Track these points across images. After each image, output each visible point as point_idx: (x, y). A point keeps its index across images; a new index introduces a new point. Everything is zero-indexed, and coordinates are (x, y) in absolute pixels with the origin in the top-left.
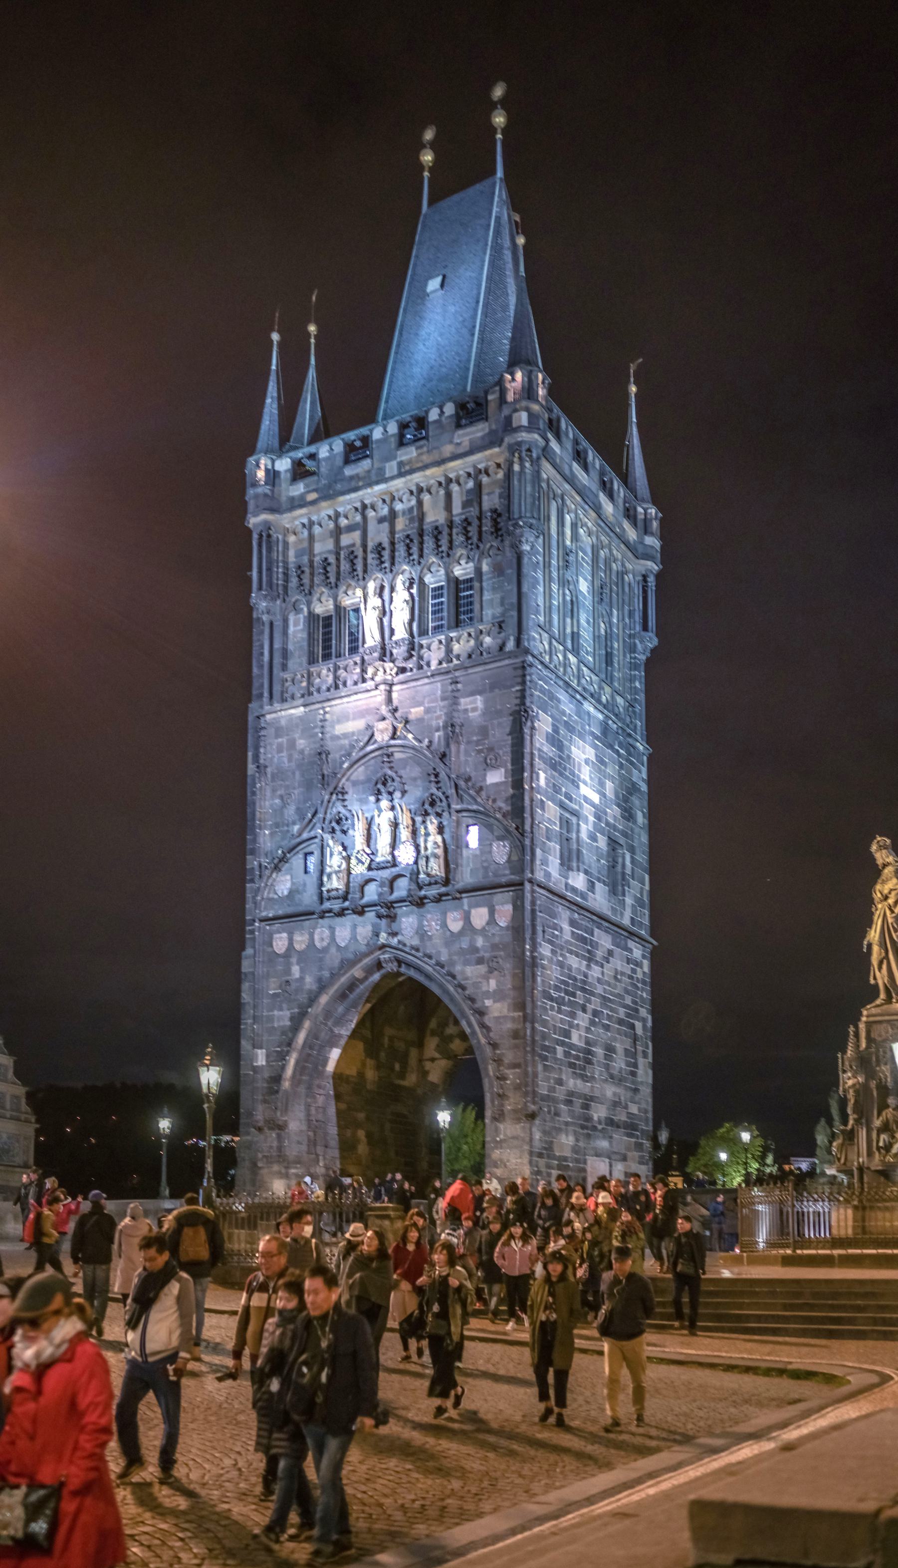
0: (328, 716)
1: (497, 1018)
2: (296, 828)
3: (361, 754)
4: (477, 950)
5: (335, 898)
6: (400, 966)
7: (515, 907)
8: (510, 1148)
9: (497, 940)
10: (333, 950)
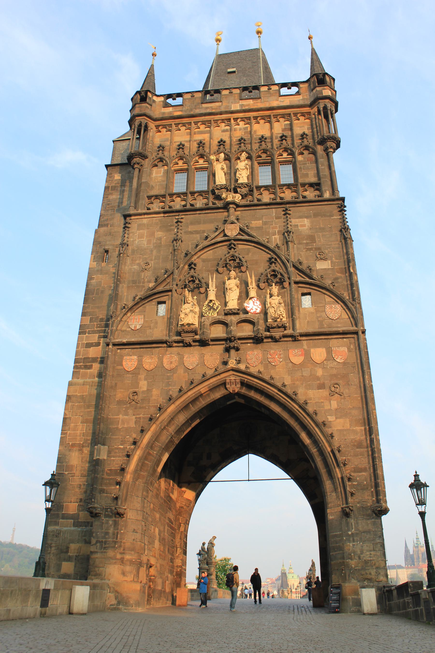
0: (182, 220)
1: (340, 431)
2: (151, 285)
3: (213, 241)
4: (318, 378)
5: (187, 332)
6: (241, 388)
7: (349, 350)
8: (364, 542)
9: (334, 372)
10: (181, 371)
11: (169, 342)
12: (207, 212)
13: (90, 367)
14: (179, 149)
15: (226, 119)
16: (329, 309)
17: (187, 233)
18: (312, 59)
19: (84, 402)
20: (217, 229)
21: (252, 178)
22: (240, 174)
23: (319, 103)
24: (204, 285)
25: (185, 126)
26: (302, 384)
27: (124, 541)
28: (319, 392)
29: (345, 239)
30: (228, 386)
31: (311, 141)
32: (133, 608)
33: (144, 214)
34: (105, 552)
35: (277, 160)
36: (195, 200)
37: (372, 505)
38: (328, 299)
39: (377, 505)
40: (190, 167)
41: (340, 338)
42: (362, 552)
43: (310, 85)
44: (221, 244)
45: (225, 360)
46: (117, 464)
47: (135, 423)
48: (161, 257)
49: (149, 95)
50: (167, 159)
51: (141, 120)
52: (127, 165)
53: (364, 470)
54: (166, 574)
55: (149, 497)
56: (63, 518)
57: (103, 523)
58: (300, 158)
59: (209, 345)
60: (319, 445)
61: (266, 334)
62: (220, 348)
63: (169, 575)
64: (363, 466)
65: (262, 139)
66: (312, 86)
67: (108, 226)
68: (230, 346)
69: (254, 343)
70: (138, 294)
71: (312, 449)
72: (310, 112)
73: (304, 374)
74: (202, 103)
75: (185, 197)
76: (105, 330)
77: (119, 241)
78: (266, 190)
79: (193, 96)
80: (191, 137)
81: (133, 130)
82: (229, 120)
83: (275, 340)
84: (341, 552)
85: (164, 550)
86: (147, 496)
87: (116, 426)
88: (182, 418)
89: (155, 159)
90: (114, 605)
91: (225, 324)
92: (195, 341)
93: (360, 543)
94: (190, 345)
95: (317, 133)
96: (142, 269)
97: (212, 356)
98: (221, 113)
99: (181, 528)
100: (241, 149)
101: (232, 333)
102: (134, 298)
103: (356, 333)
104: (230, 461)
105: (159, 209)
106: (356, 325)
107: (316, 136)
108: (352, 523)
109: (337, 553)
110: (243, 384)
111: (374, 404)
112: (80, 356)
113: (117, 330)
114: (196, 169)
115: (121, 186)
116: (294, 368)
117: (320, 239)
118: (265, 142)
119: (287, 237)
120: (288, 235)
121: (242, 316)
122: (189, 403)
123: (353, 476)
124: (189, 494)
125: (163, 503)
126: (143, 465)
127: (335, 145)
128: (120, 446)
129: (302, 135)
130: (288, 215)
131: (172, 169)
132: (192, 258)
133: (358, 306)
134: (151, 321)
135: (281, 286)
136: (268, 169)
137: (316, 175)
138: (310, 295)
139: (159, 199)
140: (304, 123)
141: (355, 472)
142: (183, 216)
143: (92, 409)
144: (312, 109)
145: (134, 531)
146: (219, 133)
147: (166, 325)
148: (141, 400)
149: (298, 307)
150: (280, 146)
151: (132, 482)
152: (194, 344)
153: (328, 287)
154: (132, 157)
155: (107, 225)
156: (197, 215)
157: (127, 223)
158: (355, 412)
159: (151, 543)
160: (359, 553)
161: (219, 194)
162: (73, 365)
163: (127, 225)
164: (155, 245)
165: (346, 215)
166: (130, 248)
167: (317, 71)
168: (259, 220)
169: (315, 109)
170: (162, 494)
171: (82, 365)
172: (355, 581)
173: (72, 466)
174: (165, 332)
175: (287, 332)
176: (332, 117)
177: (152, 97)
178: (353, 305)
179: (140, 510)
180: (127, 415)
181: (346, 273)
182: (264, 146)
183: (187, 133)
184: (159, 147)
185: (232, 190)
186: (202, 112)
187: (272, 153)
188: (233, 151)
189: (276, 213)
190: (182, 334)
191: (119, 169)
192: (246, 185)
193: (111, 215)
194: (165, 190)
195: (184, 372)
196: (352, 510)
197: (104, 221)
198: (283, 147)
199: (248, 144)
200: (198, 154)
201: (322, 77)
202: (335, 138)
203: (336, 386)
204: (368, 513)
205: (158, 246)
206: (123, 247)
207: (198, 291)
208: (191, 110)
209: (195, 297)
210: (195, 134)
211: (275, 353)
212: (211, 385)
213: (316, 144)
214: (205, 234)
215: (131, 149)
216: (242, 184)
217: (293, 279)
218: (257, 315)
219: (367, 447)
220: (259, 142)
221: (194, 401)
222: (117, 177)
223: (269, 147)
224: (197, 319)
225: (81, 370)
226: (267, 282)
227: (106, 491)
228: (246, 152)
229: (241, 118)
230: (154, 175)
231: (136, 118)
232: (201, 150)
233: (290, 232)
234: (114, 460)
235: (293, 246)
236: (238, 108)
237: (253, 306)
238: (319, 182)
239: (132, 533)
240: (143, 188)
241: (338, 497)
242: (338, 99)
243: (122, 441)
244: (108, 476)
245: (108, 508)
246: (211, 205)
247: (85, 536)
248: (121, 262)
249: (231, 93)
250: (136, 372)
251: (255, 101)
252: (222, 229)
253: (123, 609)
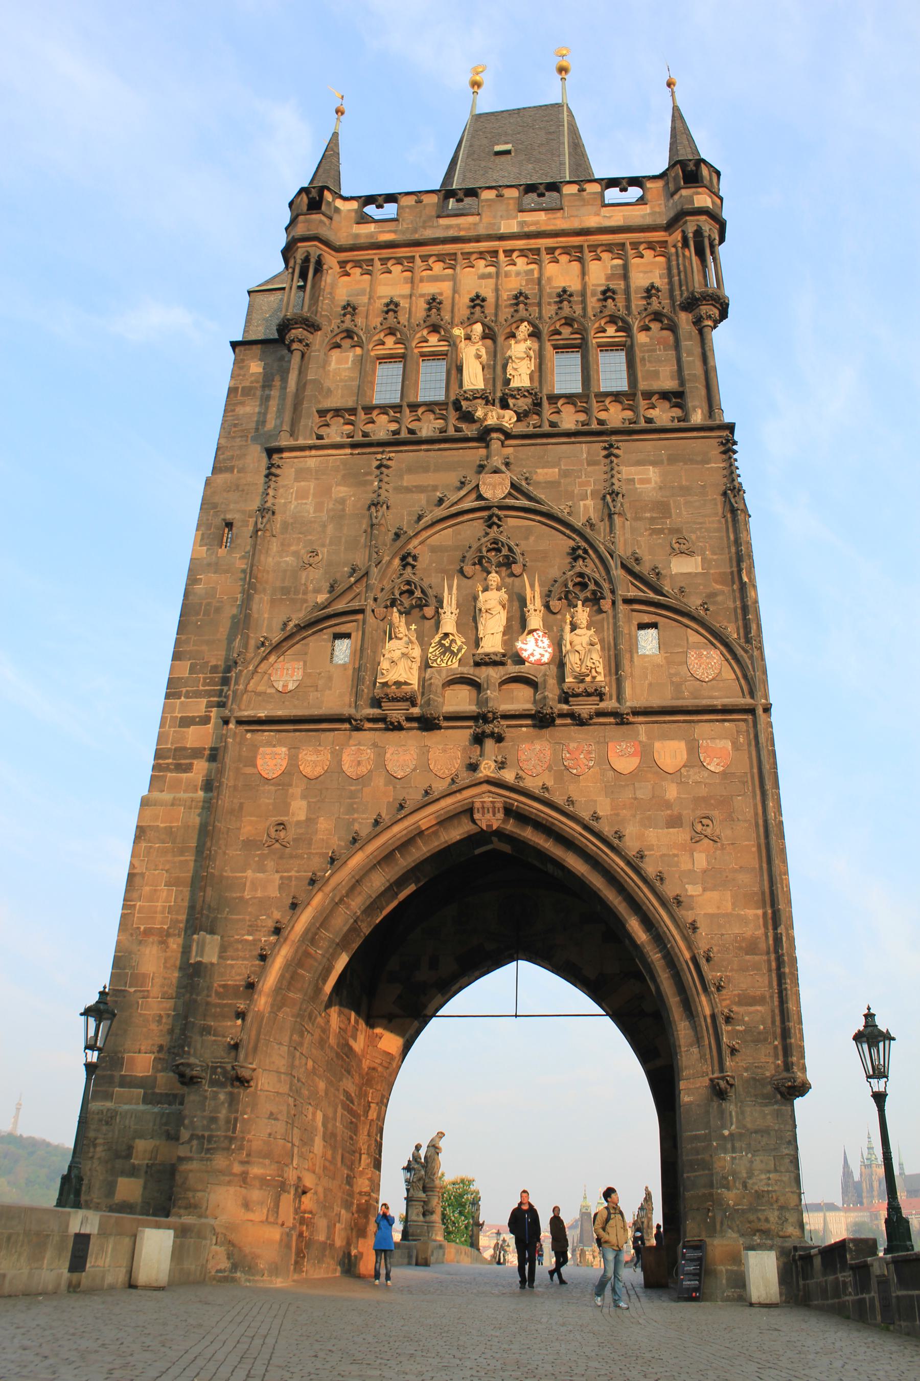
0: (389, 463)
2: (321, 598)
3: (454, 510)
4: (668, 805)
5: (395, 699)
6: (505, 821)
7: (736, 746)
8: (755, 1152)
9: (703, 791)
10: (379, 781)
11: (356, 720)
12: (442, 446)
13: (188, 768)
14: (387, 312)
15: (488, 252)
16: (696, 659)
17: (399, 490)
18: (673, 129)
19: (174, 842)
20: (463, 483)
21: (540, 376)
22: (516, 369)
23: (686, 222)
24: (432, 601)
25: (401, 264)
26: (635, 816)
27: (250, 1136)
28: (668, 833)
29: (733, 511)
30: (477, 816)
31: (666, 302)
32: (265, 1278)
33: (311, 448)
34: (208, 1159)
35: (594, 341)
36: (419, 420)
37: (774, 1076)
38: (694, 638)
39: (785, 1075)
40: (409, 351)
41: (717, 721)
42: (750, 1174)
43: (667, 184)
44: (471, 516)
45: (473, 761)
46: (239, 974)
47: (280, 888)
48: (343, 540)
49: (328, 196)
50: (361, 333)
51: (308, 249)
52: (276, 343)
53: (761, 1000)
54: (337, 1209)
55: (305, 1045)
56: (121, 1085)
57: (206, 1098)
58: (642, 338)
59: (440, 728)
60: (665, 946)
61: (561, 708)
62: (463, 736)
63: (343, 1212)
64: (758, 993)
65: (564, 295)
66: (672, 187)
67: (232, 472)
68: (483, 732)
69: (534, 726)
70: (294, 617)
71: (651, 954)
72: (666, 242)
73: (640, 795)
74: (439, 217)
75: (398, 415)
76: (222, 691)
77: (256, 504)
78: (568, 403)
79: (421, 202)
80: (412, 288)
81: (290, 270)
82: (495, 253)
83: (579, 721)
84: (707, 1172)
85: (334, 1158)
86: (301, 1044)
87: (238, 895)
88: (378, 881)
89: (335, 333)
90: (225, 1271)
91: (476, 685)
92: (409, 719)
93: (746, 1155)
94: (399, 728)
95: (681, 286)
96: (302, 564)
97: (446, 752)
98: (478, 239)
99: (370, 1112)
100: (518, 316)
101: (490, 704)
102: (285, 625)
103: (751, 711)
104: (477, 973)
105: (342, 437)
106: (752, 694)
107: (677, 292)
108: (731, 1113)
109: (697, 1174)
110: (509, 811)
111: (784, 861)
112: (167, 744)
113: (246, 690)
114: (423, 355)
115: (264, 387)
116: (618, 781)
117: (680, 510)
118: (569, 302)
119: (611, 505)
120: (613, 500)
121: (512, 669)
122: (394, 850)
123: (737, 1013)
124: (390, 1042)
125: (335, 1059)
126: (294, 976)
127: (717, 312)
128: (246, 937)
129: (647, 289)
130: (613, 458)
131: (372, 354)
132: (409, 543)
133: (756, 653)
134: (320, 674)
135: (595, 608)
136: (575, 359)
137: (676, 374)
138: (656, 628)
139: (343, 417)
140: (652, 263)
141: (740, 1004)
142: (393, 455)
143: (190, 858)
144: (670, 235)
145: (272, 1116)
146: (473, 279)
147: (350, 682)
148: (294, 840)
149: (631, 652)
150: (601, 312)
151: (270, 1012)
152: (408, 725)
153: (694, 613)
154: (288, 326)
155: (230, 469)
156: (422, 453)
157: (273, 465)
158: (745, 878)
159: (307, 1142)
160: (745, 1175)
161: (470, 409)
162: (151, 762)
163: (273, 470)
164: (331, 514)
165: (736, 460)
166: (278, 518)
167: (685, 154)
168: (553, 467)
169: (678, 235)
170: (332, 1041)
171: (171, 763)
172: (735, 1235)
173: (144, 976)
174: (348, 699)
175: (605, 705)
176: (713, 253)
177: (333, 201)
178: (746, 651)
179: (284, 1073)
180: (263, 873)
181: (733, 583)
182: (566, 310)
183: (405, 278)
184: (344, 308)
185: (497, 401)
186: (437, 235)
187: (584, 326)
188: (502, 318)
189: (588, 453)
190: (383, 704)
191: (259, 352)
192: (528, 391)
193: (240, 447)
194: (355, 398)
195: (386, 785)
196: (731, 1085)
197: (224, 460)
198: (607, 313)
199: (533, 304)
200: (428, 324)
201: (694, 168)
202: (718, 297)
203: (705, 821)
204: (765, 1091)
205: (338, 517)
206: (263, 517)
207: (421, 614)
208: (415, 231)
209: (413, 627)
210: (421, 281)
212: (442, 812)
213: (677, 308)
214: (438, 494)
215: (287, 310)
216: (518, 389)
217: (620, 592)
218: (542, 667)
219: (768, 953)
220: (556, 302)
221: (405, 845)
222: (256, 368)
223: (577, 313)
224: (416, 673)
225: (169, 774)
226: (566, 598)
227: (215, 1030)
228: (529, 323)
229: (521, 250)
230: (333, 365)
231: (299, 245)
232: (433, 316)
233: (618, 494)
234: (232, 966)
235: (624, 523)
236: (515, 229)
237: (536, 648)
238: (681, 389)
239: (266, 1121)
240: (308, 392)
241: (702, 1056)
242: (725, 215)
243: (250, 926)
244: (220, 998)
245: (217, 1067)
246: (451, 432)
247: (166, 1124)
248: (258, 547)
249: (500, 196)
250: (283, 782)
251: (550, 216)
252: (473, 484)
253: (243, 1279)
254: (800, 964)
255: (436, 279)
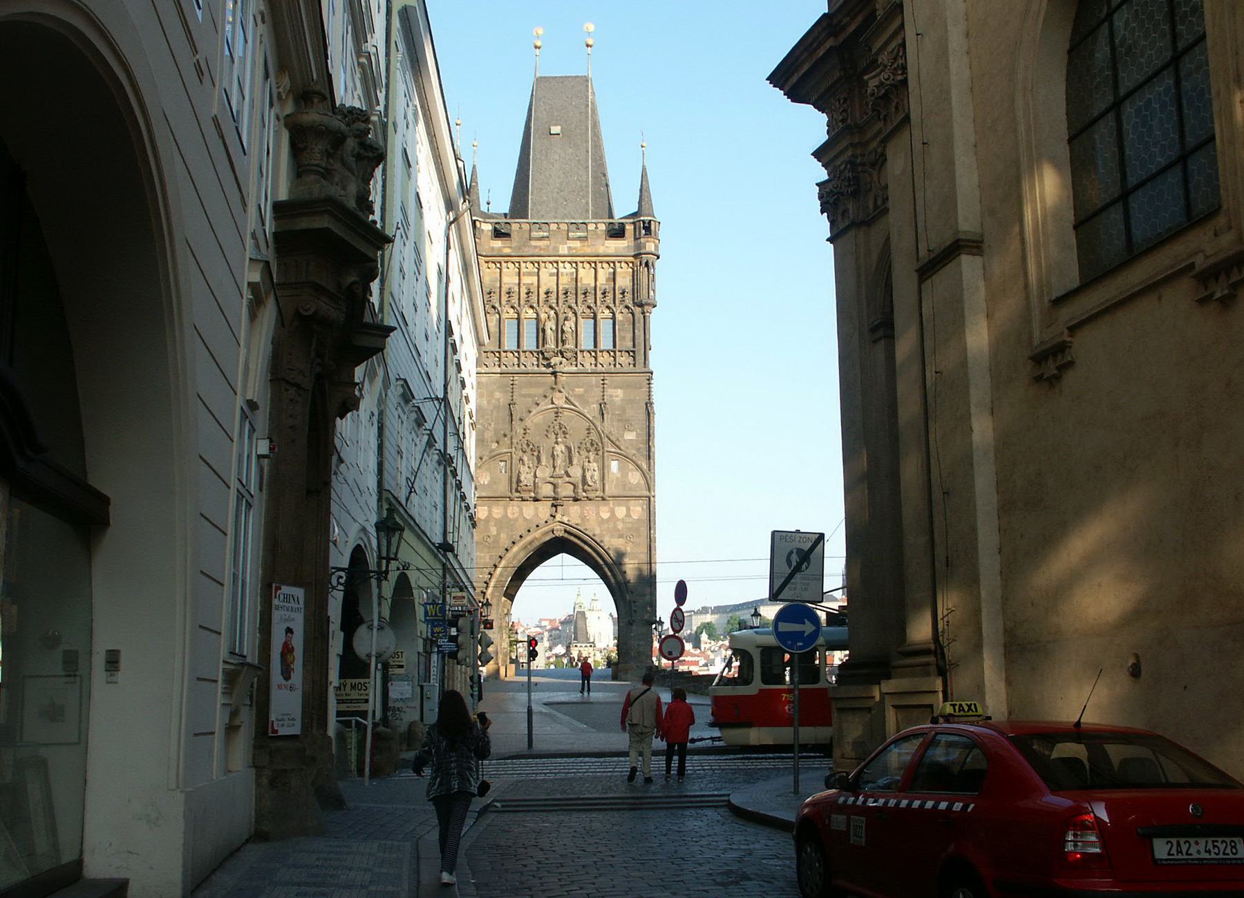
10: (520, 520)
38: (631, 466)
58: (619, 317)
97: (544, 509)
205: (497, 408)
211: (589, 508)
221: (530, 543)
236: (566, 252)
250: (487, 520)
254: (658, 585)
255: (530, 274)
